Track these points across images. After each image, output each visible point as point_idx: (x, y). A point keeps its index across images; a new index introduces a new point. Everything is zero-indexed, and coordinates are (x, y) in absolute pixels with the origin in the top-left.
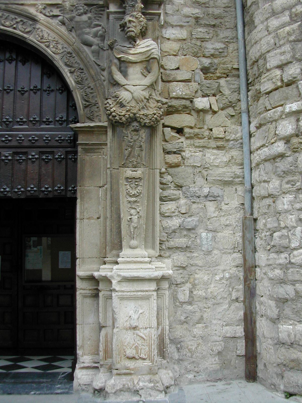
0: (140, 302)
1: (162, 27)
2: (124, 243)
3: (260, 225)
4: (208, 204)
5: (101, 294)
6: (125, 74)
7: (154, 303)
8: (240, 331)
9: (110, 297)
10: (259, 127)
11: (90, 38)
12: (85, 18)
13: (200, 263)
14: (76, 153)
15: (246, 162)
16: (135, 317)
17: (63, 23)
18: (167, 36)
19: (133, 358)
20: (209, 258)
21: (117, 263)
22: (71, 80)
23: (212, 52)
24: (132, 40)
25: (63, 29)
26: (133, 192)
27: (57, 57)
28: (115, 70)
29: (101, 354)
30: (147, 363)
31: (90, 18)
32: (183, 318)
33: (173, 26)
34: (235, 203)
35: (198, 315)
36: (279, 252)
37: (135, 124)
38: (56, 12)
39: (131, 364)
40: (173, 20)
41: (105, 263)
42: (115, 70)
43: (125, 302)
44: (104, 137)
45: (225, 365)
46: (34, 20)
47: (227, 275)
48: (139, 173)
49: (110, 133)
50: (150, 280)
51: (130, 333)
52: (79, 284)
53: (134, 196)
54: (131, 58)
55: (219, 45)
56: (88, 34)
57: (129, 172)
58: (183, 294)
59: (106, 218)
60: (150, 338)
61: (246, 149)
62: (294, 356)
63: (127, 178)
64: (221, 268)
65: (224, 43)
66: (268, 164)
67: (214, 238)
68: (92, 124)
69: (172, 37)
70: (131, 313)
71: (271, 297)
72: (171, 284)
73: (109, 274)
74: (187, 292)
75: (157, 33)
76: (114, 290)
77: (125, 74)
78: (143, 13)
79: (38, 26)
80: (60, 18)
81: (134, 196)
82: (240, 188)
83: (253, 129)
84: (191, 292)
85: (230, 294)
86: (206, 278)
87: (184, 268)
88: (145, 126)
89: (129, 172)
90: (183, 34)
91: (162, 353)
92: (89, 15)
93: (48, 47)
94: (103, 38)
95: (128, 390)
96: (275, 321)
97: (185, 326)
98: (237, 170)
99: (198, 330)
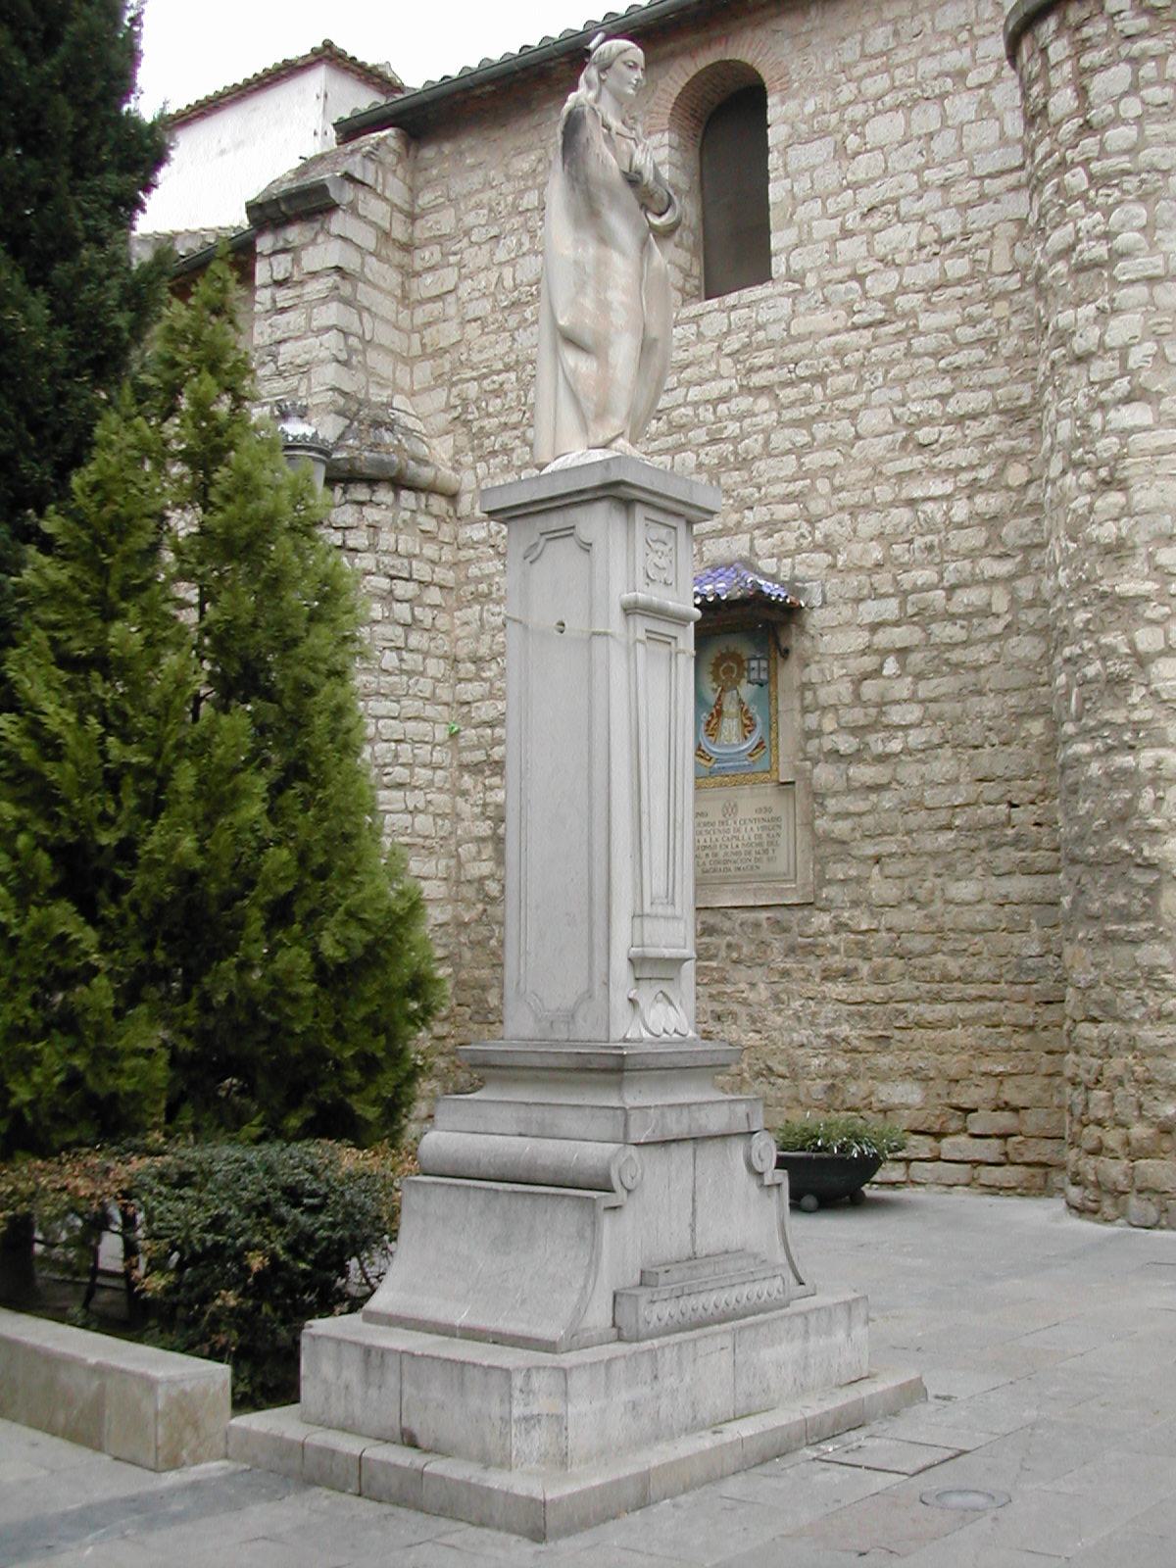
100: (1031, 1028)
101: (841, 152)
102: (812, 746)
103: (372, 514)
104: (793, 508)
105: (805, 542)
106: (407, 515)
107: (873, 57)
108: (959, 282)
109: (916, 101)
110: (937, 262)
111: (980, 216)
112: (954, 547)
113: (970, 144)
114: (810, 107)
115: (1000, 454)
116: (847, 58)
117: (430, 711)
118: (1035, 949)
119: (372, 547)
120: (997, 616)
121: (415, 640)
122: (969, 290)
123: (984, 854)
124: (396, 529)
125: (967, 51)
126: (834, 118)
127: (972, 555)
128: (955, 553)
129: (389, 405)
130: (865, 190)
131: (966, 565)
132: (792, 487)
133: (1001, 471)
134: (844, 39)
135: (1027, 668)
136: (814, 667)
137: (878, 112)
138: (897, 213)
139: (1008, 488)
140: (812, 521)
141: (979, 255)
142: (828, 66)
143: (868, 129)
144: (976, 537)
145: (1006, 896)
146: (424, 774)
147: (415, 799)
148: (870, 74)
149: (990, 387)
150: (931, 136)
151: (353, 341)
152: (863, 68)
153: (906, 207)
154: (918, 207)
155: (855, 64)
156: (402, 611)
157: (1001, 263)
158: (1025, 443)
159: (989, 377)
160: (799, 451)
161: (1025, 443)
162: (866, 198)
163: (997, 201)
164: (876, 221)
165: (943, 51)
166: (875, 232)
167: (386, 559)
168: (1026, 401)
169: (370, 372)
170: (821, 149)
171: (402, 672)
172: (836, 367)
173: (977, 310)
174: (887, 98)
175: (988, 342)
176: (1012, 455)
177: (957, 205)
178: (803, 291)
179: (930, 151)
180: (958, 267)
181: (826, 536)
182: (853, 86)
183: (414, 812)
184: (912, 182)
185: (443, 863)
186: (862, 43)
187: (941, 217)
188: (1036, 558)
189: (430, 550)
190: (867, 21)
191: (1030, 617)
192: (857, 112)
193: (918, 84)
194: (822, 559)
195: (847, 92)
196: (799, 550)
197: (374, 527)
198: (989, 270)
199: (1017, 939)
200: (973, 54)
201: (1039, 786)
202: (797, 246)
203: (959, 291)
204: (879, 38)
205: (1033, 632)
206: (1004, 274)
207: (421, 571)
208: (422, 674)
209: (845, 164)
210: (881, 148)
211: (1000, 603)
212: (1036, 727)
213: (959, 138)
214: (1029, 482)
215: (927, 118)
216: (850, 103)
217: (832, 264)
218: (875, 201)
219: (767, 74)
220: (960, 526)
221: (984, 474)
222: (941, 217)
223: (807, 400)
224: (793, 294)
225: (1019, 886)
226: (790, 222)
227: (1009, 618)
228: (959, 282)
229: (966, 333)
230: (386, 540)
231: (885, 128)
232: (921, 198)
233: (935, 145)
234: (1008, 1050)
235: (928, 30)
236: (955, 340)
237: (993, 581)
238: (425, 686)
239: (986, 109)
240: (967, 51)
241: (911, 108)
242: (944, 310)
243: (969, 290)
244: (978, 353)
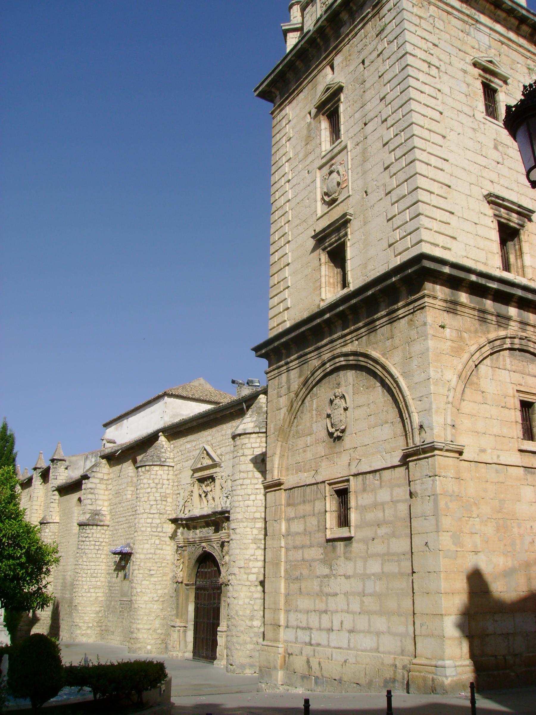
103: (92, 531)
106: (99, 531)
117: (101, 564)
119: (92, 537)
121: (99, 552)
124: (96, 533)
129: (101, 510)
146: (99, 575)
147: (97, 579)
151: (93, 500)
156: (97, 547)
167: (94, 539)
169: (97, 505)
171: (96, 557)
183: (97, 581)
185: (102, 590)
189: (103, 536)
197: (93, 533)
207: (101, 540)
208: (100, 558)
230: (95, 535)
238: (101, 560)
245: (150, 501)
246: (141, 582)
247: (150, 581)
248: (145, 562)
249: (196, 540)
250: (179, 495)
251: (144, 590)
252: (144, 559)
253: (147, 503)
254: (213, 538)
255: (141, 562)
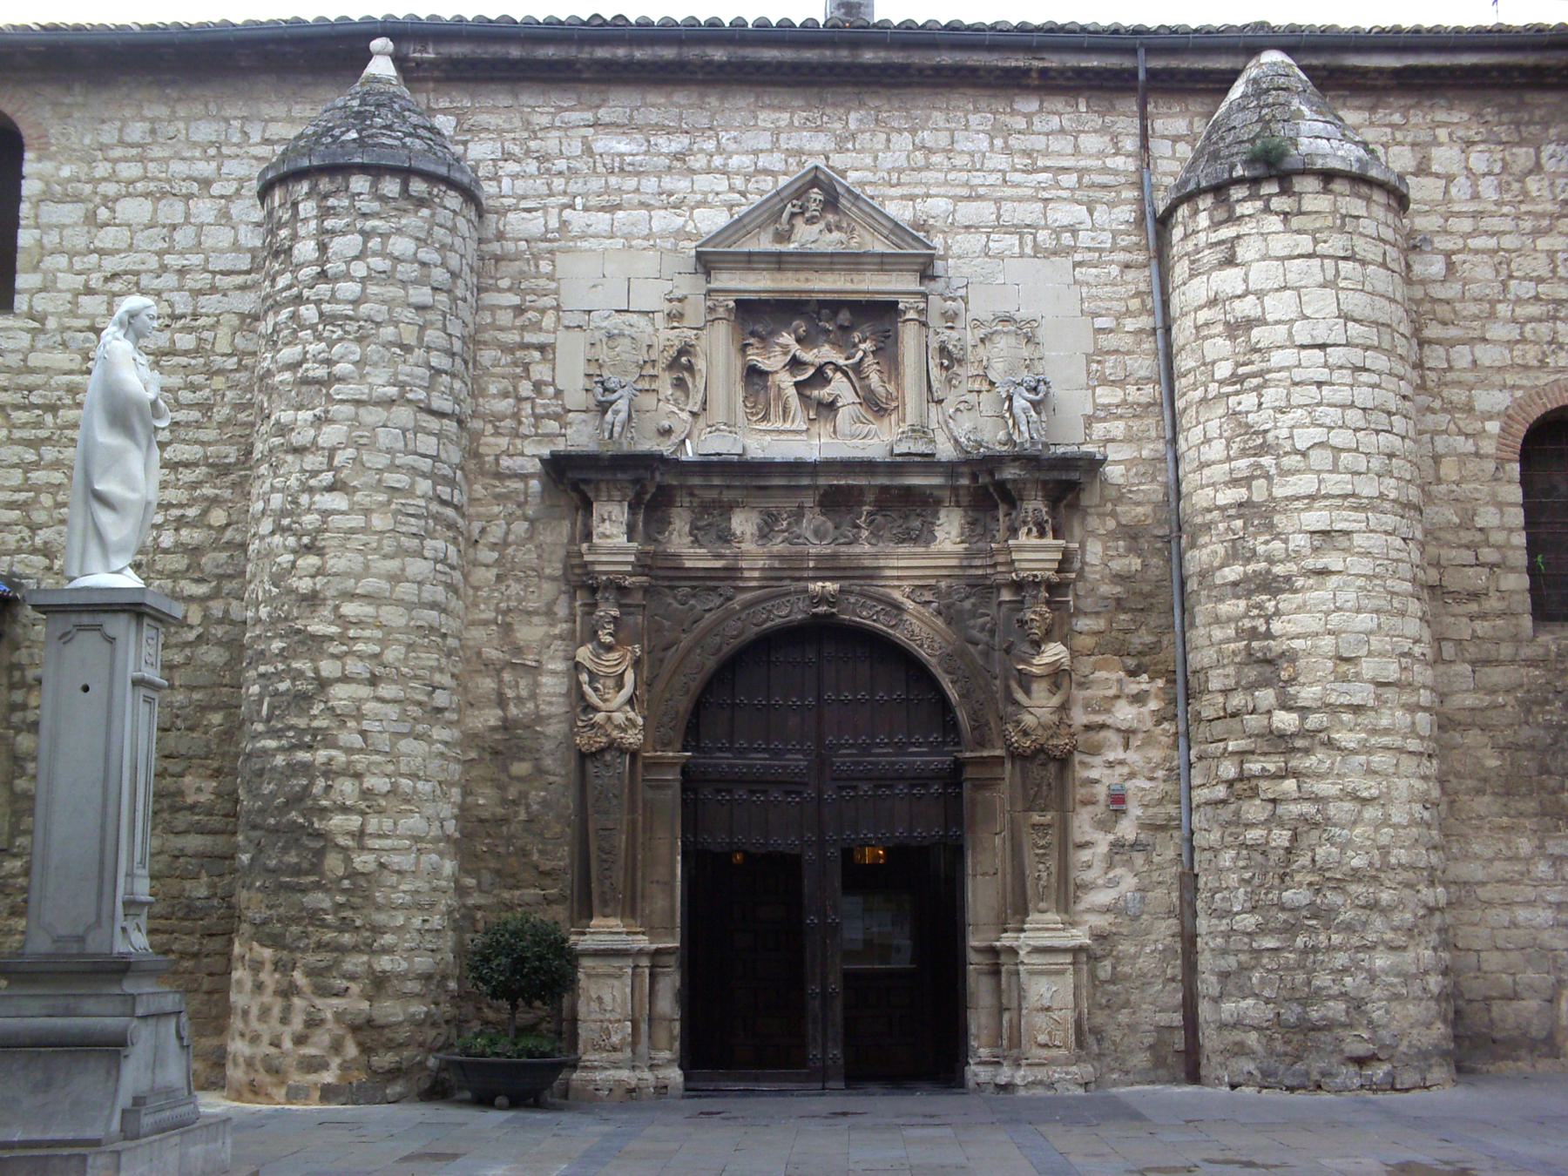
0: (1053, 978)
1: (1072, 615)
2: (1031, 906)
3: (1201, 884)
4: (1135, 854)
5: (1004, 969)
6: (1028, 692)
7: (1069, 978)
8: (1177, 1019)
9: (1017, 973)
10: (1200, 758)
11: (975, 633)
12: (967, 604)
13: (1125, 931)
14: (960, 785)
15: (1184, 801)
16: (1048, 995)
17: (939, 613)
18: (1078, 628)
19: (1045, 1046)
20: (1136, 925)
21: (1023, 930)
22: (953, 694)
23: (1140, 648)
24: (1037, 645)
25: (940, 622)
26: (1042, 843)
27: (933, 661)
28: (1014, 685)
29: (1005, 1042)
30: (1063, 1052)
31: (974, 605)
32: (1104, 1001)
33: (1086, 614)
34: (1171, 853)
35: (1122, 997)
36: (1221, 917)
37: (1042, 756)
38: (928, 596)
39: (1045, 1053)
40: (1088, 604)
41: (1006, 931)
42: (1014, 685)
43: (1036, 978)
44: (999, 770)
45: (1159, 1062)
46: (898, 607)
47: (1160, 947)
48: (1048, 817)
49: (1008, 766)
50: (1065, 951)
51: (1042, 1015)
52: (972, 957)
53: (1042, 847)
54: (1034, 670)
55: (1149, 639)
56: (973, 627)
57: (1036, 818)
58: (1105, 969)
59: (1004, 875)
60: (1066, 1021)
61: (1183, 784)
62: (1238, 1038)
63: (1034, 826)
64: (1153, 937)
65: (1156, 634)
66: (1208, 808)
67: (1143, 899)
68: (985, 754)
69: (1086, 629)
70: (1043, 990)
71: (1212, 972)
72: (1089, 957)
73: (1015, 944)
74: (1109, 968)
75: (1066, 629)
76: (1022, 963)
77: (1028, 692)
78: (1048, 603)
79: (906, 617)
80: (935, 605)
81: (1042, 847)
82: (1176, 834)
83: (1193, 759)
84: (1114, 968)
85: (1164, 972)
86: (1133, 950)
87: (1105, 938)
88: (1054, 758)
89: (1036, 818)
90: (1101, 624)
91: (1080, 1043)
92: (972, 600)
93: (921, 646)
94: (992, 632)
95: (1041, 1083)
96: (1216, 1000)
97: (1107, 1011)
98: (1171, 809)
99: (1123, 1017)
100: (195, 955)
101: (91, 219)
102: (16, 718)
104: (15, 514)
105: (25, 545)
107: (132, 146)
108: (185, 353)
109: (164, 194)
110: (167, 334)
111: (209, 303)
112: (159, 567)
113: (208, 243)
114: (66, 172)
115: (206, 498)
116: (105, 139)
118: (203, 892)
120: (191, 627)
122: (193, 362)
123: (166, 815)
125: (214, 165)
126: (88, 188)
127: (174, 575)
128: (160, 572)
130: (109, 258)
131: (169, 584)
132: (16, 496)
133: (205, 513)
134: (103, 122)
135: (213, 671)
136: (24, 651)
137: (129, 195)
138: (137, 284)
139: (210, 527)
140: (34, 528)
141: (205, 334)
142: (87, 141)
143: (119, 207)
144: (179, 562)
145: (182, 850)
148: (126, 160)
149: (202, 443)
150: (174, 227)
152: (118, 152)
153: (145, 280)
154: (157, 284)
155: (111, 147)
157: (223, 346)
158: (227, 494)
159: (203, 435)
160: (27, 467)
161: (227, 494)
162: (111, 264)
163: (225, 295)
164: (117, 286)
165: (192, 159)
166: (115, 295)
168: (232, 460)
170: (71, 213)
172: (68, 401)
173: (199, 379)
174: (138, 185)
175: (206, 407)
176: (215, 501)
177: (190, 290)
178: (43, 331)
179: (171, 237)
180: (186, 341)
181: (46, 543)
182: (109, 165)
184: (153, 263)
186: (121, 130)
187: (176, 297)
188: (228, 586)
190: (128, 113)
191: (219, 631)
192: (110, 189)
193: (168, 181)
194: (40, 561)
195: (102, 169)
196: (19, 551)
198: (212, 350)
199: (188, 885)
200: (219, 169)
201: (215, 765)
202: (41, 290)
203: (184, 360)
204: (137, 131)
205: (219, 643)
206: (223, 355)
209: (94, 230)
210: (129, 226)
211: (195, 616)
212: (216, 718)
213: (198, 236)
214: (228, 525)
215: (172, 211)
216: (104, 179)
217: (73, 314)
218: (118, 269)
219: (27, 132)
220: (166, 551)
221: (192, 512)
222: (176, 297)
223: (38, 425)
224: (34, 332)
225: (194, 842)
226: (36, 268)
227: (201, 630)
228: (185, 353)
229: (186, 396)
231: (134, 210)
232: (159, 276)
233: (178, 235)
234: (175, 973)
235: (182, 137)
236: (176, 400)
237: (191, 599)
239: (225, 217)
240: (214, 165)
241: (159, 199)
242: (170, 374)
243: (193, 362)
244: (195, 415)
245: (429, 349)
246: (393, 744)
247: (431, 742)
248: (410, 647)
249: (743, 564)
250: (537, 355)
251: (405, 783)
252: (407, 630)
253: (411, 359)
254: (895, 563)
255: (384, 643)
